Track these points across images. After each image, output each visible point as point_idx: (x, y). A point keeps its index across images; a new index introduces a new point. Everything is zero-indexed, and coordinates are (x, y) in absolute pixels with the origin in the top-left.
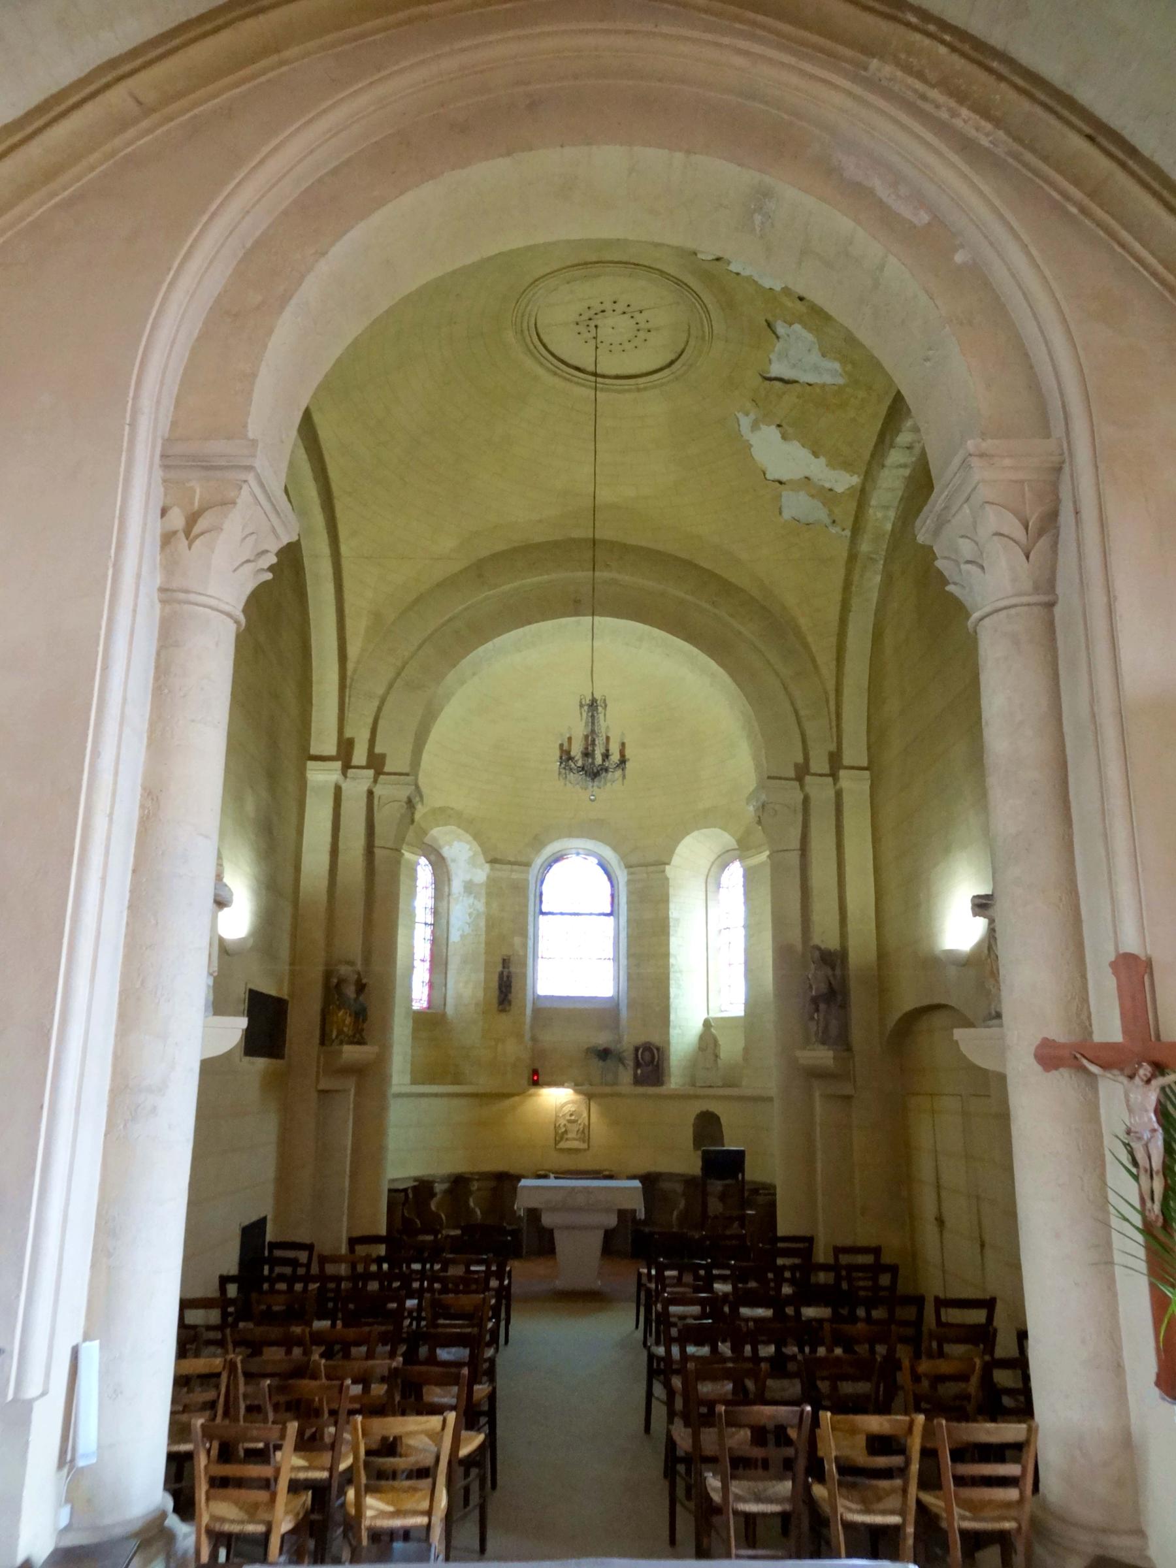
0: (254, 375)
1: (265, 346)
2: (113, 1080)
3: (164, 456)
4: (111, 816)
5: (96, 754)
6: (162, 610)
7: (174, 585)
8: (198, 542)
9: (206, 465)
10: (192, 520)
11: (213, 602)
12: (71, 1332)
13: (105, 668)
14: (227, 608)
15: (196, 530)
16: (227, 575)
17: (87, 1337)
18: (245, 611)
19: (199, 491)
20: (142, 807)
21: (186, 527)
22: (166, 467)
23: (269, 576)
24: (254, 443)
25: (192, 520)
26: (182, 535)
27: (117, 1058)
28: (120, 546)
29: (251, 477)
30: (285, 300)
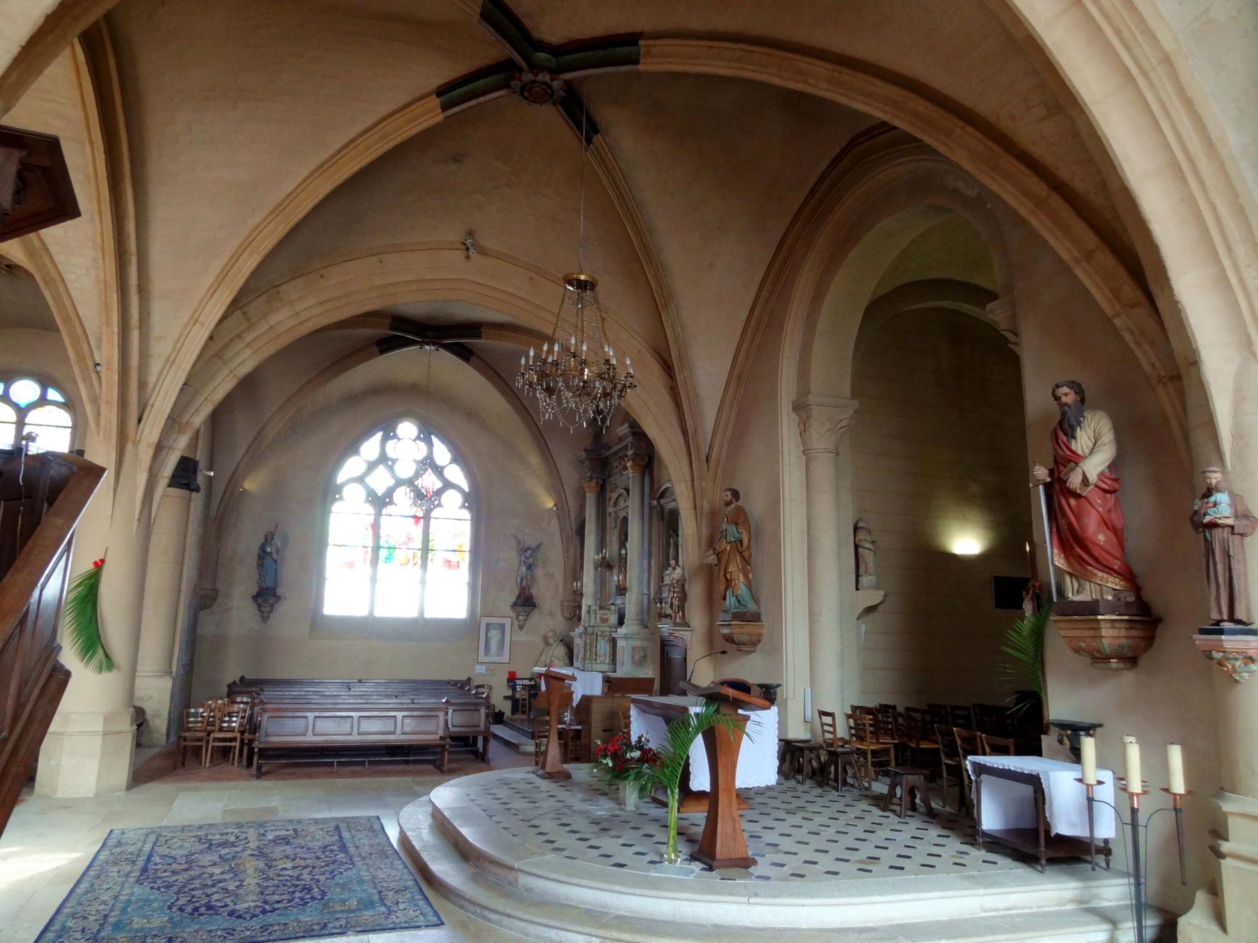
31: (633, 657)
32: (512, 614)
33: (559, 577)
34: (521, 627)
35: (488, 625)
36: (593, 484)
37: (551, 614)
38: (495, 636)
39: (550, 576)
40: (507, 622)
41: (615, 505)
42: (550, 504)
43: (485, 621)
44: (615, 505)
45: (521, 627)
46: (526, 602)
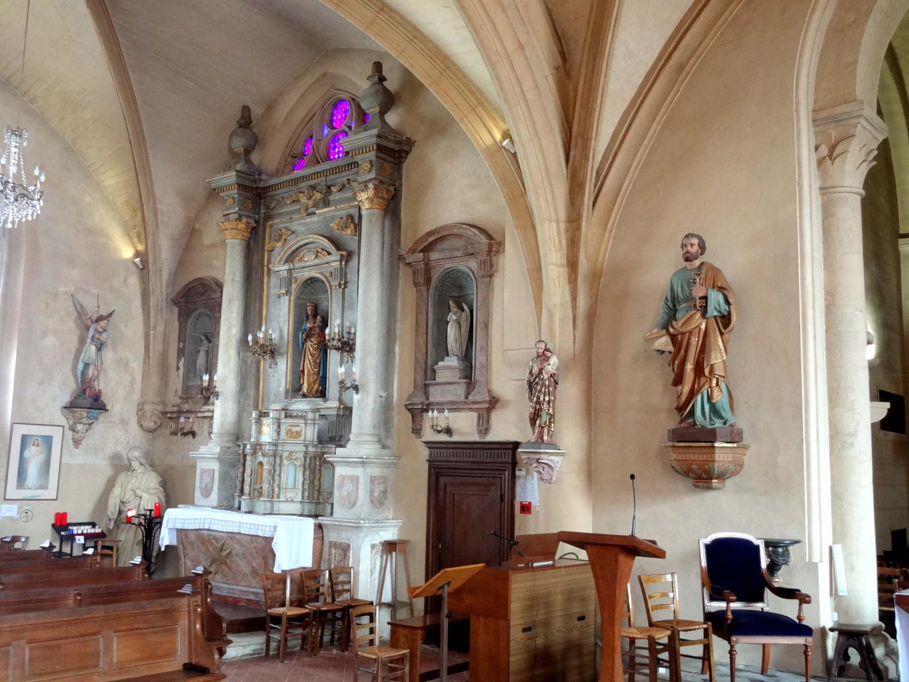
0: (856, 62)
1: (860, 43)
2: (830, 430)
3: (814, 121)
4: (814, 307)
5: (803, 279)
6: (822, 199)
7: (827, 185)
8: (836, 161)
9: (836, 120)
10: (832, 149)
11: (849, 189)
12: (828, 541)
13: (802, 236)
14: (854, 190)
15: (835, 154)
16: (852, 173)
17: (834, 543)
18: (864, 188)
19: (834, 134)
20: (826, 300)
21: (829, 153)
22: (815, 126)
23: (875, 163)
24: (861, 102)
25: (832, 149)
26: (827, 158)
27: (831, 420)
28: (800, 175)
29: (862, 120)
30: (868, 14)
31: (371, 492)
32: (63, 421)
33: (136, 366)
34: (77, 443)
35: (25, 439)
36: (242, 226)
37: (123, 422)
38: (35, 456)
39: (123, 364)
40: (56, 434)
41: (290, 259)
42: (127, 252)
43: (20, 431)
44: (290, 259)
45: (77, 443)
46: (88, 402)
